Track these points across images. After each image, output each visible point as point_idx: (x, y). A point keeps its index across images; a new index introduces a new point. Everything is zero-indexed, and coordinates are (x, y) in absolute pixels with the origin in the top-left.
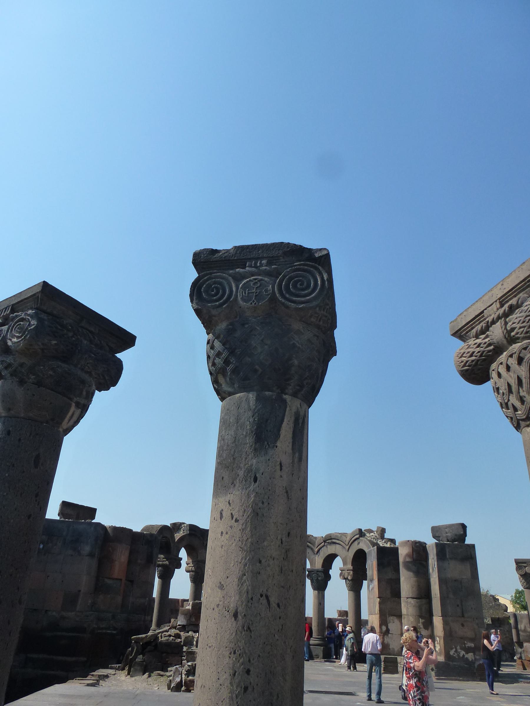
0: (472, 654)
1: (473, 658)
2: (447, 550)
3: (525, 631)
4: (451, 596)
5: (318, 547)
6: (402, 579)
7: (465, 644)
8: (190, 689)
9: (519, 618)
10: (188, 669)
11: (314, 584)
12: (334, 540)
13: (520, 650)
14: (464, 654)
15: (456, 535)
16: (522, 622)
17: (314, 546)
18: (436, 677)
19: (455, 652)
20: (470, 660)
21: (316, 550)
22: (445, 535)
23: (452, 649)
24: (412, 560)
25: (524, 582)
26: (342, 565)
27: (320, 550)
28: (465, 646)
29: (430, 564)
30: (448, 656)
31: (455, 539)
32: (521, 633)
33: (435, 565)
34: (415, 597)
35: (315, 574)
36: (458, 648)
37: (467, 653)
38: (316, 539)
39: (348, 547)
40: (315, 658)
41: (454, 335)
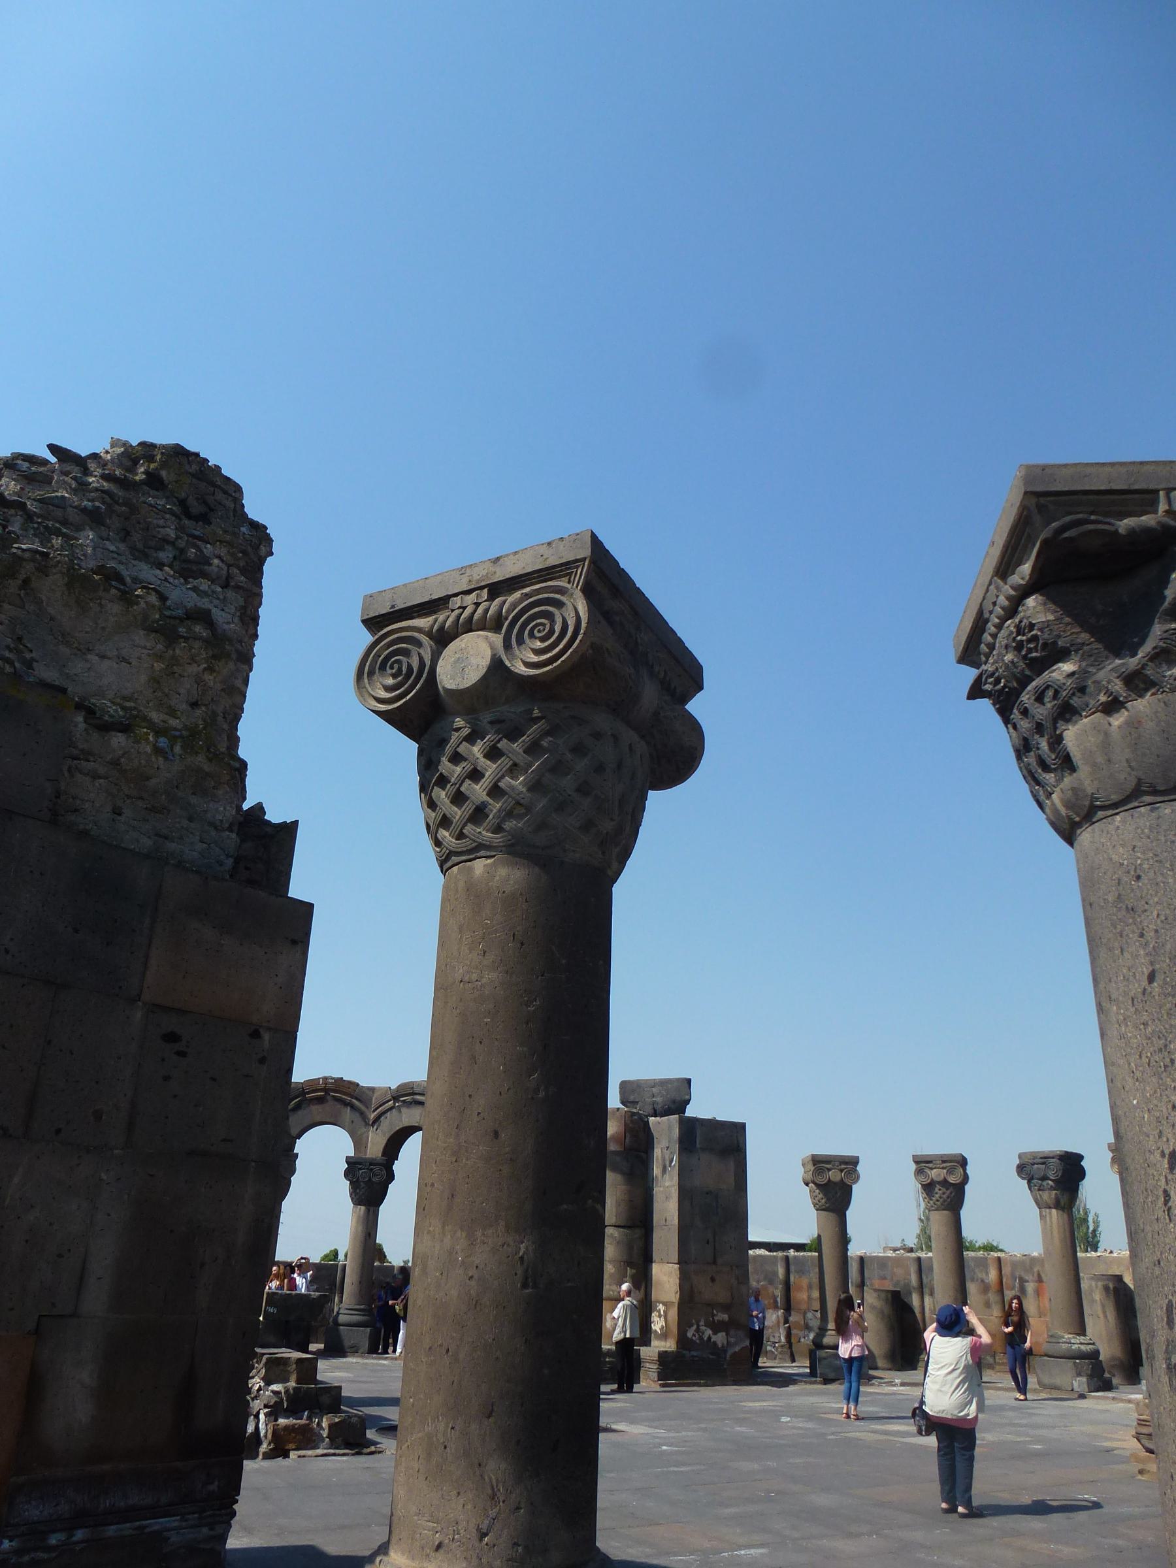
0: (724, 1334)
1: (725, 1342)
5: (378, 1111)
7: (713, 1315)
8: (287, 1448)
10: (276, 1402)
11: (360, 1191)
12: (418, 1097)
14: (710, 1335)
15: (674, 1102)
17: (367, 1108)
18: (659, 1382)
19: (695, 1331)
20: (720, 1346)
21: (372, 1116)
22: (650, 1100)
24: (622, 1149)
25: (822, 1199)
27: (383, 1118)
28: (713, 1319)
29: (657, 1159)
30: (682, 1340)
31: (669, 1108)
33: (671, 1161)
34: (622, 1225)
35: (364, 1169)
36: (702, 1323)
37: (715, 1333)
38: (373, 1093)
40: (349, 1354)
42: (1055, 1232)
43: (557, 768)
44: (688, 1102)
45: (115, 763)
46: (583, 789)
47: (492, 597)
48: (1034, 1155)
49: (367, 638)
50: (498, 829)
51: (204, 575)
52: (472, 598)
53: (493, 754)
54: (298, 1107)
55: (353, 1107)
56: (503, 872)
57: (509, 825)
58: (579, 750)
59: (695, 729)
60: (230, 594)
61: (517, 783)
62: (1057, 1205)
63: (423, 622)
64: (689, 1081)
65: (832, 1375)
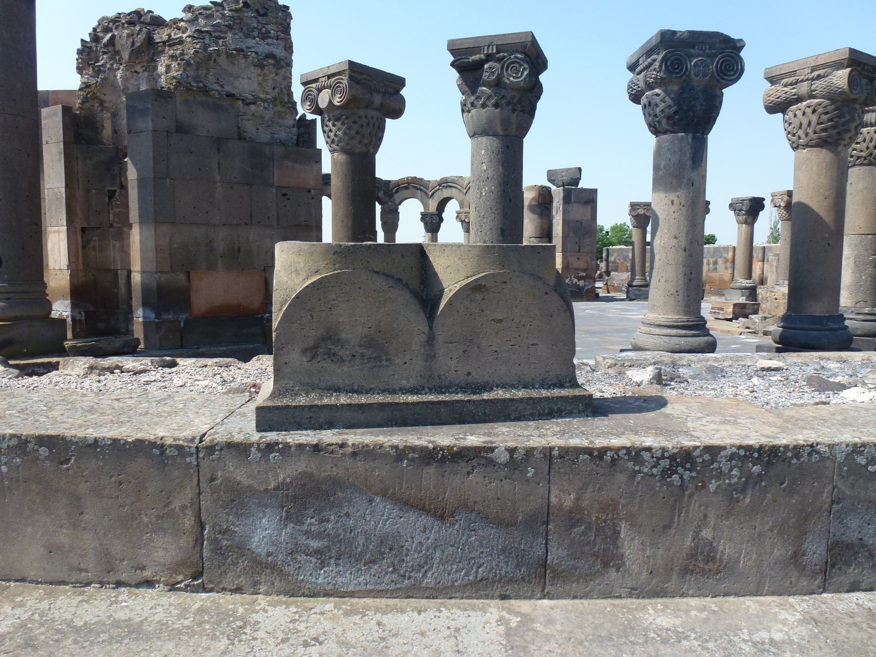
2: (573, 194)
3: (614, 262)
4: (572, 234)
6: (526, 221)
9: (610, 252)
13: (607, 278)
15: (572, 179)
16: (612, 256)
21: (430, 193)
23: (567, 278)
26: (458, 209)
32: (610, 264)
39: (465, 191)
41: (766, 79)
42: (743, 234)
43: (349, 128)
44: (580, 179)
45: (254, 115)
46: (357, 133)
47: (328, 79)
48: (738, 199)
49: (303, 88)
50: (338, 146)
51: (270, 37)
52: (324, 79)
53: (334, 125)
54: (397, 192)
55: (421, 190)
56: (340, 156)
57: (340, 144)
58: (355, 122)
59: (402, 101)
60: (279, 42)
61: (340, 133)
62: (746, 222)
63: (314, 85)
64: (580, 169)
65: (633, 298)
